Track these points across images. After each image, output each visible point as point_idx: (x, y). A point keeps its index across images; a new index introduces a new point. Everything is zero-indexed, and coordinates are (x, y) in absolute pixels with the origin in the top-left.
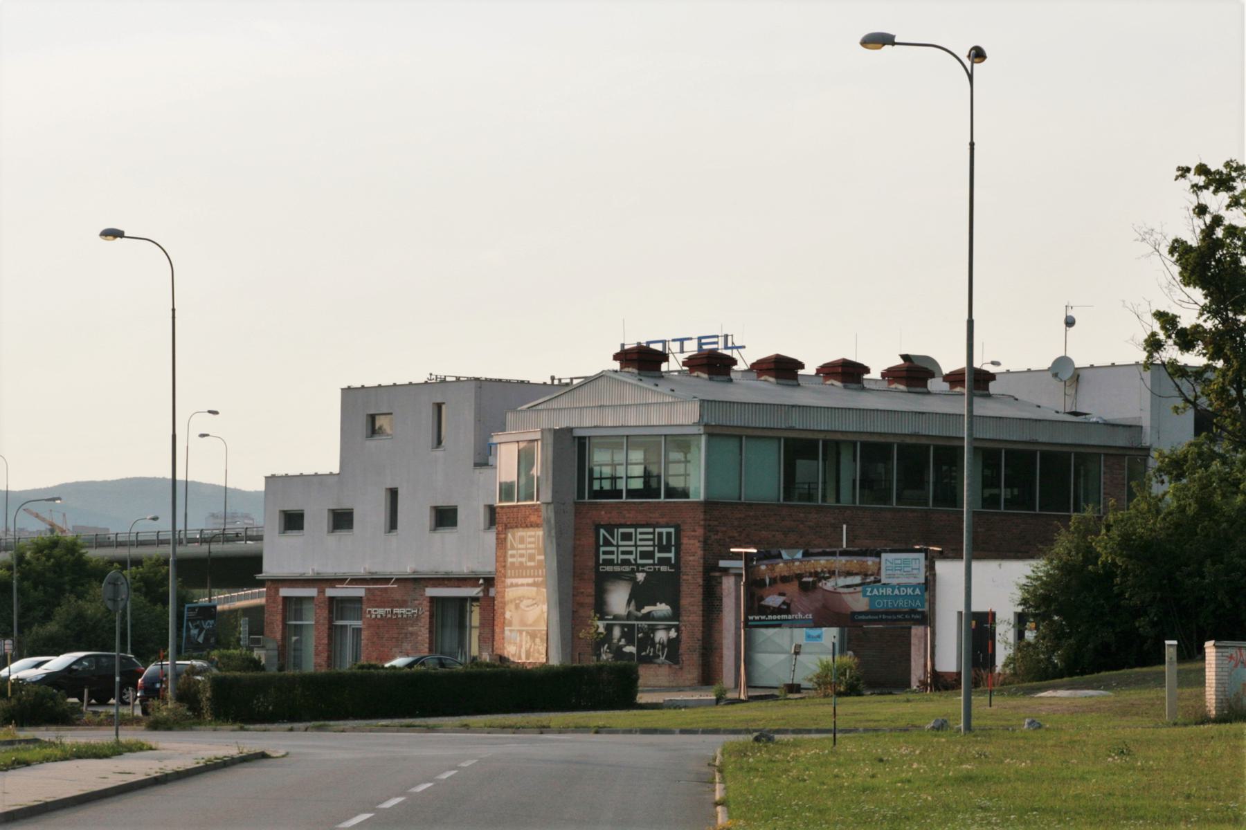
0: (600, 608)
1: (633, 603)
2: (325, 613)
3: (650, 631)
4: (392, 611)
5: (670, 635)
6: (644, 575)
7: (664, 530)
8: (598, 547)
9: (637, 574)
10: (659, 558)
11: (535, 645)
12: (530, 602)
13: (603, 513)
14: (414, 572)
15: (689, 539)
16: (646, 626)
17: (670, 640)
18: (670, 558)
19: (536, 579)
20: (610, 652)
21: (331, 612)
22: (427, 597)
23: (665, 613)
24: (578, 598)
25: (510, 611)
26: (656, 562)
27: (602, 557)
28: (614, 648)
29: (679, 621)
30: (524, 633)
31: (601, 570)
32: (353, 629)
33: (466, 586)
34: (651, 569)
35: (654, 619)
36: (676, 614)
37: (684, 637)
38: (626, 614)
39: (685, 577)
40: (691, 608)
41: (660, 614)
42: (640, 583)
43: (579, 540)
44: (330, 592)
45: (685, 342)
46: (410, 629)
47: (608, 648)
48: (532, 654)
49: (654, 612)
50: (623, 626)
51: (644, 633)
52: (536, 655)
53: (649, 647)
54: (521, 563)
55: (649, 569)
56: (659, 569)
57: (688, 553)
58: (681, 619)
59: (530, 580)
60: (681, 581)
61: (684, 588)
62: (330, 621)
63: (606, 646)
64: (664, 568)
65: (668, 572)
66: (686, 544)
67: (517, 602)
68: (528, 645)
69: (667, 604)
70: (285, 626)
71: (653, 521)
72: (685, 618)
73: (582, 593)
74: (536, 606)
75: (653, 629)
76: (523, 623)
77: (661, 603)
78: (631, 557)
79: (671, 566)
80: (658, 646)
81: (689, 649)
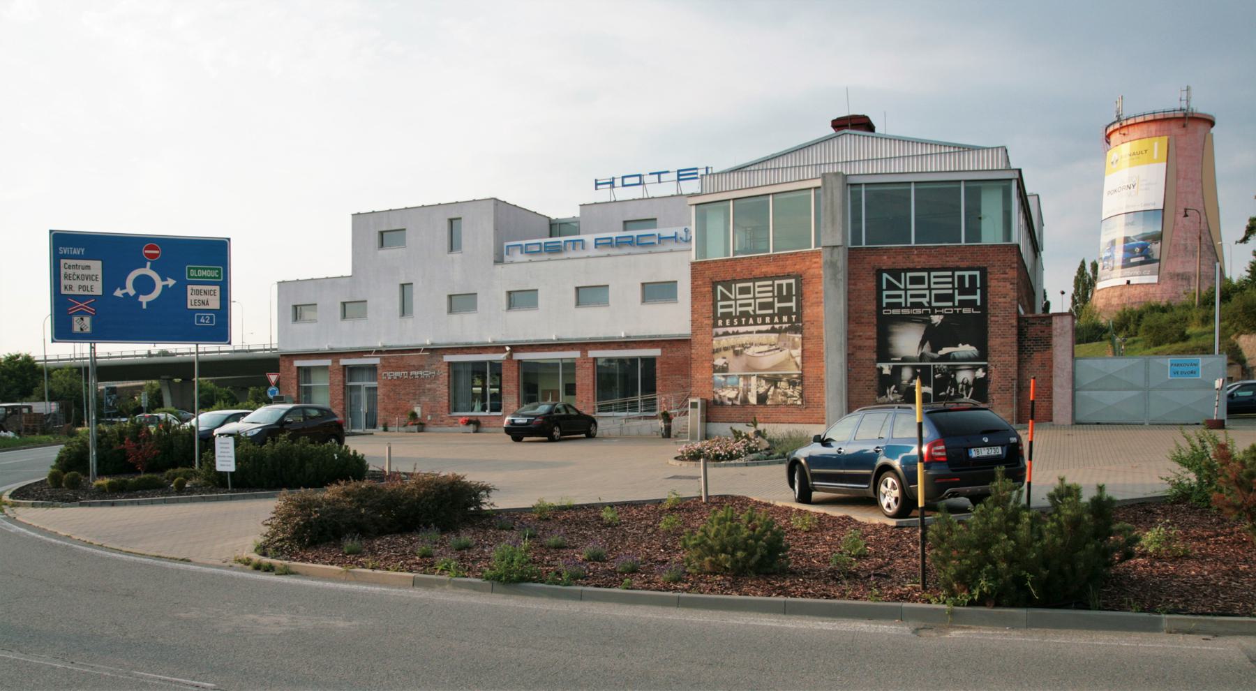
0: (884, 351)
1: (927, 344)
2: (340, 377)
3: (951, 372)
4: (409, 374)
5: (976, 375)
6: (942, 317)
7: (967, 274)
8: (879, 290)
9: (932, 316)
10: (959, 301)
13: (885, 257)
14: (432, 344)
15: (998, 282)
16: (945, 367)
17: (975, 380)
18: (975, 301)
20: (898, 393)
21: (344, 376)
23: (970, 354)
24: (854, 341)
26: (957, 304)
27: (885, 301)
28: (904, 389)
29: (986, 361)
30: (754, 379)
31: (884, 313)
32: (366, 388)
33: (487, 353)
34: (951, 311)
35: (955, 360)
36: (983, 354)
37: (994, 377)
38: (919, 355)
39: (993, 318)
40: (1003, 349)
41: (962, 355)
42: (936, 325)
43: (855, 284)
44: (344, 362)
45: (662, 175)
46: (428, 386)
47: (895, 389)
48: (770, 397)
49: (955, 354)
50: (914, 368)
51: (942, 374)
53: (949, 387)
55: (947, 311)
56: (961, 311)
57: (997, 295)
58: (989, 359)
60: (989, 322)
61: (992, 329)
62: (344, 382)
63: (893, 387)
64: (966, 311)
65: (972, 314)
66: (995, 286)
69: (971, 345)
70: (299, 387)
71: (950, 264)
72: (994, 359)
73: (860, 336)
74: (779, 351)
75: (955, 370)
77: (963, 345)
78: (925, 301)
79: (976, 308)
80: (960, 386)
81: (1000, 388)
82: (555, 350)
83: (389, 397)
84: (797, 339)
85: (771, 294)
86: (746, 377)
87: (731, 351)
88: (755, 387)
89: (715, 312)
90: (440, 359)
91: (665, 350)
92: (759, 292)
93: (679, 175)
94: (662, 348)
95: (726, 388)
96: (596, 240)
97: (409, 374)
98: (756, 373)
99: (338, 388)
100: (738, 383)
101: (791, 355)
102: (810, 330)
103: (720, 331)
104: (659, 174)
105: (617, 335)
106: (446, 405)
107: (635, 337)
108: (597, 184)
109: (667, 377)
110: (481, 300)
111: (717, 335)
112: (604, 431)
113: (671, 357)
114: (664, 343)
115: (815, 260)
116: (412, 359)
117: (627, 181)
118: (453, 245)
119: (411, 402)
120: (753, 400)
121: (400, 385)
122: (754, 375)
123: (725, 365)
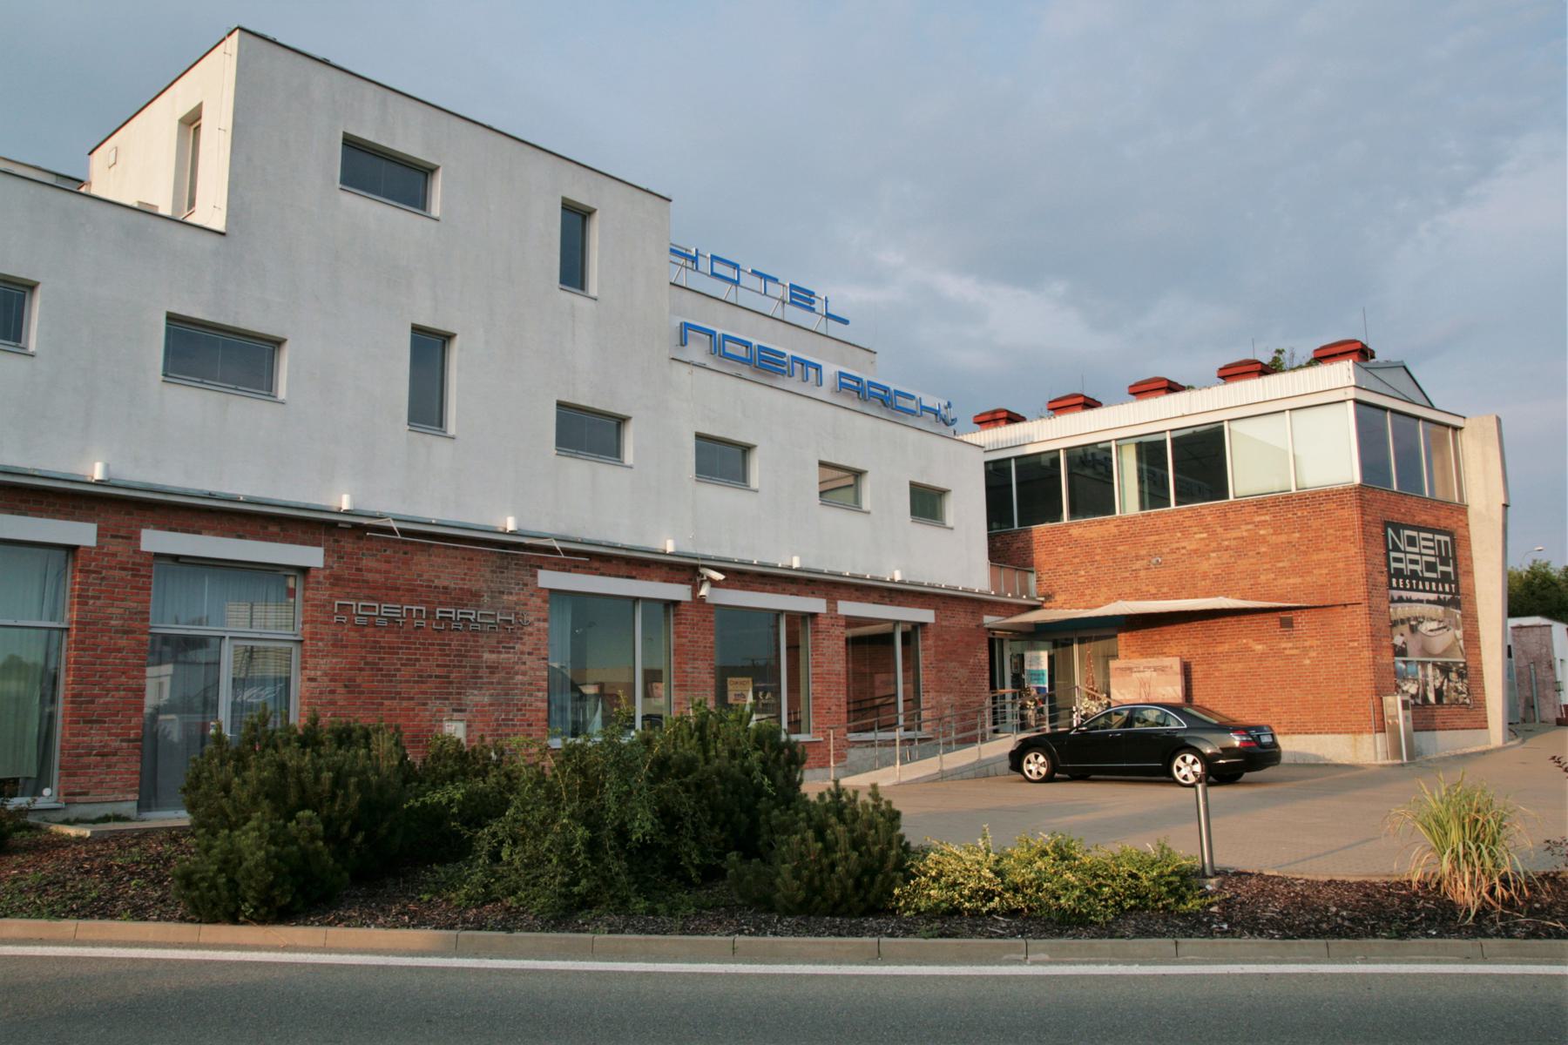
4: (431, 613)
11: (1449, 680)
12: (1434, 625)
19: (1442, 596)
22: (542, 589)
25: (1402, 635)
30: (1430, 667)
33: (649, 578)
52: (1453, 694)
54: (1414, 572)
59: (1433, 597)
67: (1413, 623)
68: (1438, 684)
76: (1425, 651)
82: (784, 592)
83: (351, 688)
85: (1432, 552)
86: (1424, 664)
89: (1388, 565)
90: (528, 579)
91: (938, 612)
93: (792, 295)
94: (936, 609)
95: (1408, 680)
96: (841, 374)
97: (431, 613)
99: (123, 642)
101: (1455, 637)
102: (1465, 606)
103: (1396, 594)
105: (881, 575)
106: (542, 715)
107: (911, 584)
109: (941, 665)
110: (631, 440)
111: (1393, 601)
113: (946, 626)
115: (1460, 517)
116: (444, 572)
117: (720, 269)
118: (573, 273)
119: (434, 705)
120: (1432, 698)
121: (393, 650)
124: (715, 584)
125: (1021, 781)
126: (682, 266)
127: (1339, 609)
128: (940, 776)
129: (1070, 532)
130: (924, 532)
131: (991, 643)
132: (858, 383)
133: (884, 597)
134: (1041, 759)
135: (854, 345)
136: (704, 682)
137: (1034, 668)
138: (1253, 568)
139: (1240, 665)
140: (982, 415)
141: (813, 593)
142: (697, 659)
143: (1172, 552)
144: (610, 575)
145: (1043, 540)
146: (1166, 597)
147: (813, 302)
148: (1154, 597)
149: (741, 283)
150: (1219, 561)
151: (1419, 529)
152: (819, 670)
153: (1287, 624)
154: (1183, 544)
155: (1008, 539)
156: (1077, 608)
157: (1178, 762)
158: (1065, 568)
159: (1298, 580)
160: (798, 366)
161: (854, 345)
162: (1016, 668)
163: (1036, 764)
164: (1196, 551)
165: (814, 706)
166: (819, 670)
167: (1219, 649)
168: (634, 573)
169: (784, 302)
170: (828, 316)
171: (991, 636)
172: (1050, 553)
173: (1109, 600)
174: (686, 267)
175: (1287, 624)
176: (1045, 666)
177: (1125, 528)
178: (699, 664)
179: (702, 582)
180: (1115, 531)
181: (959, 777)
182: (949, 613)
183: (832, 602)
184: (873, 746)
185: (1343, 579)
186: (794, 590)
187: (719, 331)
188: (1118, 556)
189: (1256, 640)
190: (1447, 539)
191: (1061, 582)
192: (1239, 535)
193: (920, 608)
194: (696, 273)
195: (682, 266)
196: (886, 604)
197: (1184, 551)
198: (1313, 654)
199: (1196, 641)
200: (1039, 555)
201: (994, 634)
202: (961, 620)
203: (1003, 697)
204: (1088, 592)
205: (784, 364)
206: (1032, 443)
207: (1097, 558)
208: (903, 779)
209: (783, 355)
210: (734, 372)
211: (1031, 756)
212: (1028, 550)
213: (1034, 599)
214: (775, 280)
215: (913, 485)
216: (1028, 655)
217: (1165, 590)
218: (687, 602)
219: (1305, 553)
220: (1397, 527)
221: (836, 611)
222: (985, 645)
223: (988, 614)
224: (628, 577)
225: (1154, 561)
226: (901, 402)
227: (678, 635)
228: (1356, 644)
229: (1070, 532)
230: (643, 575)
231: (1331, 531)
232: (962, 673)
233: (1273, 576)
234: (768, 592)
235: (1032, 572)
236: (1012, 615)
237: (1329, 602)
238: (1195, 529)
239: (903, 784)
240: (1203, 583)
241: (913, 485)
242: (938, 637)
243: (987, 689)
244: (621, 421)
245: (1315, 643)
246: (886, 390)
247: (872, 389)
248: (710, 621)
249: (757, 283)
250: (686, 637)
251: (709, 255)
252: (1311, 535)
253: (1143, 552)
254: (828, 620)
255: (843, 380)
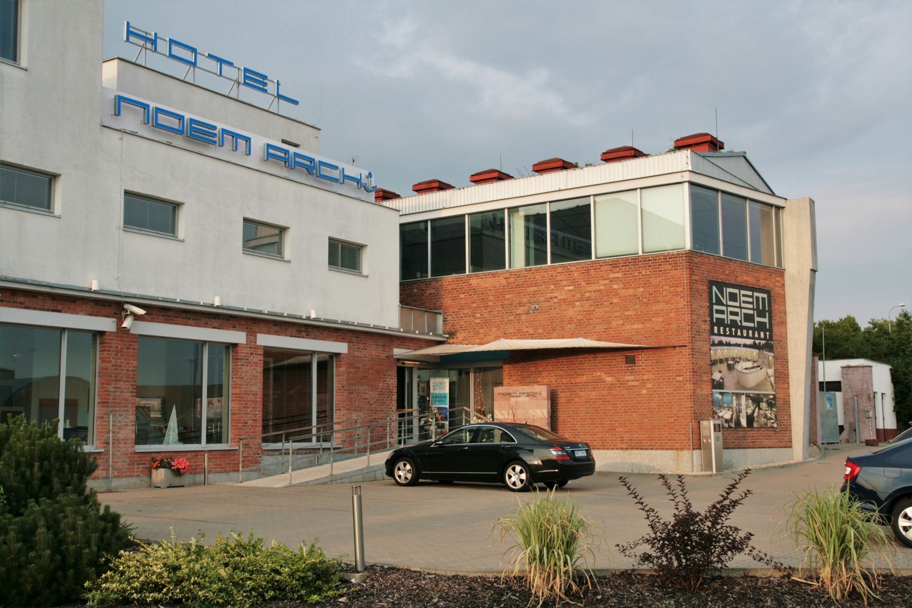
11: (760, 409)
12: (749, 364)
19: (757, 342)
25: (720, 372)
30: (743, 397)
33: (75, 312)
48: (756, 419)
52: (763, 420)
54: (734, 323)
59: (749, 342)
67: (731, 362)
68: (750, 411)
74: (759, 368)
76: (739, 385)
82: (206, 325)
84: (770, 358)
85: (751, 306)
86: (738, 395)
87: (725, 364)
88: (745, 407)
89: (711, 316)
92: (744, 302)
93: (246, 77)
94: (349, 342)
95: (724, 408)
96: (269, 146)
98: (745, 392)
100: (732, 403)
101: (768, 374)
102: (777, 349)
103: (717, 339)
104: (221, 61)
105: (298, 314)
107: (326, 321)
108: (129, 33)
109: (352, 388)
111: (714, 344)
112: (377, 473)
113: (358, 357)
114: (351, 334)
115: (777, 279)
117: (177, 51)
120: (744, 422)
122: (743, 394)
123: (721, 381)
124: (137, 317)
125: (394, 485)
126: (142, 47)
127: (670, 350)
128: (330, 479)
129: (471, 282)
130: (342, 279)
131: (401, 372)
132: (285, 154)
133: (302, 331)
134: (408, 467)
135: (300, 122)
136: (128, 400)
137: (438, 392)
138: (607, 315)
139: (594, 393)
140: (419, 184)
141: (234, 327)
142: (120, 381)
143: (547, 300)
144: (35, 309)
145: (449, 287)
146: (541, 337)
147: (266, 84)
148: (532, 337)
149: (198, 65)
150: (581, 309)
151: (740, 287)
152: (237, 391)
153: (631, 361)
154: (555, 295)
155: (423, 286)
156: (473, 344)
157: (509, 471)
158: (465, 311)
159: (640, 326)
160: (228, 138)
161: (300, 122)
162: (423, 391)
163: (404, 471)
164: (564, 300)
165: (232, 420)
166: (237, 391)
167: (579, 380)
168: (60, 308)
169: (239, 83)
170: (279, 97)
171: (401, 365)
172: (454, 299)
173: (497, 338)
174: (146, 49)
175: (631, 361)
176: (447, 391)
177: (512, 280)
178: (121, 384)
179: (126, 316)
180: (504, 282)
181: (348, 480)
182: (361, 346)
183: (252, 334)
184: (281, 454)
185: (674, 326)
186: (216, 324)
187: (153, 105)
188: (506, 302)
189: (608, 374)
190: (765, 296)
191: (462, 322)
192: (598, 288)
193: (335, 341)
194: (156, 54)
195: (142, 47)
196: (303, 337)
197: (555, 300)
198: (649, 385)
199: (562, 373)
200: (447, 301)
201: (404, 363)
202: (373, 351)
203: (410, 414)
204: (482, 331)
205: (215, 135)
206: (444, 209)
207: (490, 304)
208: (294, 482)
209: (215, 128)
210: (165, 140)
211: (401, 464)
212: (436, 296)
213: (440, 336)
214: (231, 64)
215: (330, 239)
216: (432, 381)
217: (540, 331)
218: (112, 332)
219: (646, 304)
220: (721, 285)
221: (256, 342)
222: (394, 373)
223: (398, 347)
224: (53, 311)
225: (532, 307)
226: (325, 171)
227: (103, 360)
228: (681, 378)
229: (471, 282)
230: (70, 309)
231: (666, 287)
232: (372, 395)
233: (621, 322)
234: (191, 325)
235: (441, 314)
236: (421, 348)
237: (663, 345)
238: (565, 283)
239: (295, 486)
240: (569, 326)
241: (330, 239)
242: (350, 365)
243: (394, 408)
244: (53, 177)
245: (651, 376)
246: (311, 160)
247: (297, 159)
248: (134, 349)
249: (214, 66)
250: (110, 362)
251: (168, 39)
252: (652, 290)
253: (525, 300)
254: (248, 350)
255: (271, 151)
